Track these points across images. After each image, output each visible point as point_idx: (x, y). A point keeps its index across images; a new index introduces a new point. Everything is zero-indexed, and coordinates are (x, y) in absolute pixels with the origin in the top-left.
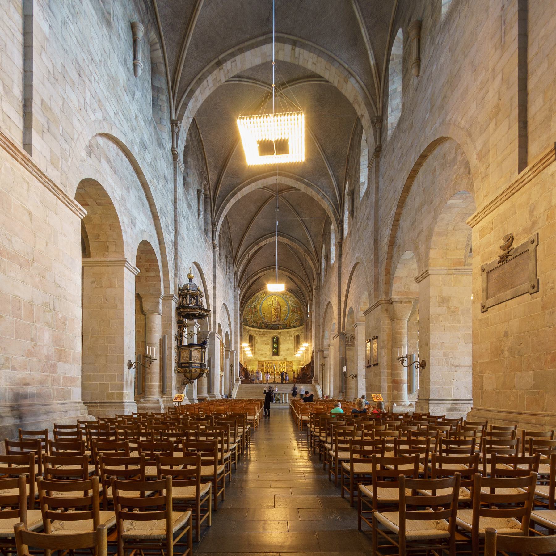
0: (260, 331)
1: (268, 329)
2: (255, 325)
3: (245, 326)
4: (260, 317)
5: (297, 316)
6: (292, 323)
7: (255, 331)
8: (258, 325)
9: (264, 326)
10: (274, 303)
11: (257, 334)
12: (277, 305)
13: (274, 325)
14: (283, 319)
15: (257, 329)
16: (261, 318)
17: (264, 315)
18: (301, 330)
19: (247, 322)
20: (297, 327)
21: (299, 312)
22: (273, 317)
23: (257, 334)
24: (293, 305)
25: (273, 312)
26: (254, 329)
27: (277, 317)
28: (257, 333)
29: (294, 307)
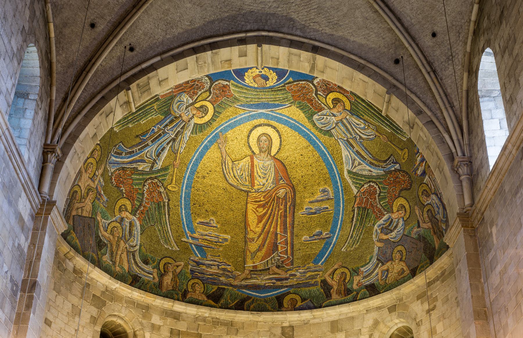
0: (176, 316)
1: (226, 307)
2: (146, 277)
3: (80, 262)
4: (179, 242)
5: (386, 229)
6: (356, 271)
7: (146, 309)
8: (168, 280)
9: (200, 288)
10: (258, 172)
11: (154, 328)
12: (276, 180)
13: (256, 288)
14: (306, 258)
15: (158, 302)
16: (185, 248)
17: (201, 230)
18: (421, 297)
19: (100, 244)
20: (388, 288)
21: (401, 201)
22: (253, 247)
23: (154, 328)
24: (365, 169)
25: (252, 218)
26: (136, 294)
27: (275, 247)
28: (156, 319)
29: (370, 178)
